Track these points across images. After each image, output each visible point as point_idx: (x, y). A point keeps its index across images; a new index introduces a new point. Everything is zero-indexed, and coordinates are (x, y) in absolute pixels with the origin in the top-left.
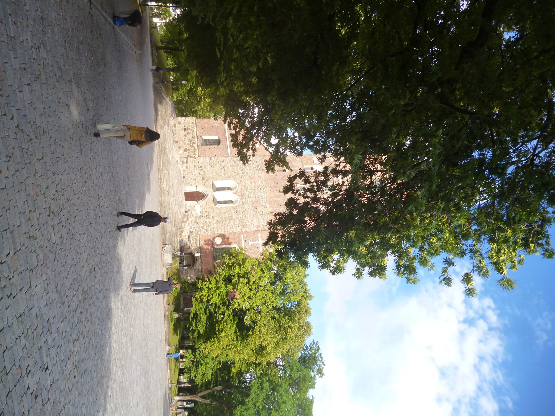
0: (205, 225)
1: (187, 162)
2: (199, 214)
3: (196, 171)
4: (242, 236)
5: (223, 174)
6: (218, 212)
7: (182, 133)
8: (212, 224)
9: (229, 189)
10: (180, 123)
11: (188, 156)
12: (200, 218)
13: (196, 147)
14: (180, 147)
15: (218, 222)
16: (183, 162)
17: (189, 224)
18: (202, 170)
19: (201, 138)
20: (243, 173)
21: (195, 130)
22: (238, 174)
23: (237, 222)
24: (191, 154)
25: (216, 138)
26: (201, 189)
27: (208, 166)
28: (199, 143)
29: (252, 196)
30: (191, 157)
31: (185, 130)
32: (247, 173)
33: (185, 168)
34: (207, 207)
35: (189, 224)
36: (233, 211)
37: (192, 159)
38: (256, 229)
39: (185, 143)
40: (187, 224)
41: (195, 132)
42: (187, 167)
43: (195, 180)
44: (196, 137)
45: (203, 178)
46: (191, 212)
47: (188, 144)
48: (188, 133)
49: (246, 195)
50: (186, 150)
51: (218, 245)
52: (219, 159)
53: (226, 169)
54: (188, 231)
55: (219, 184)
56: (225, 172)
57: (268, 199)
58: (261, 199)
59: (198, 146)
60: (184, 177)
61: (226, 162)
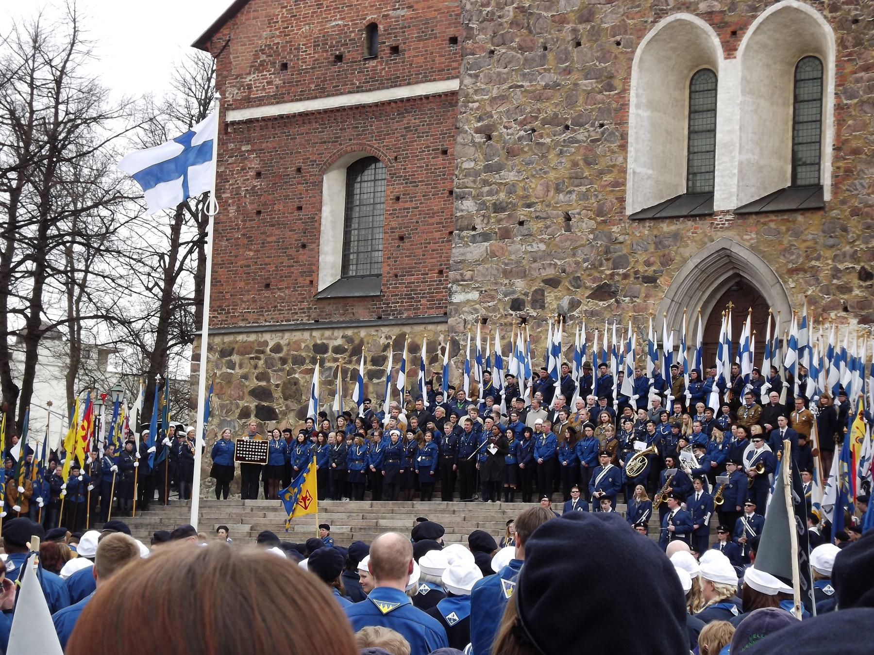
13: (383, 336)
18: (538, 301)
21: (272, 340)
25: (333, 185)
27: (517, 248)
28: (362, 313)
34: (825, 267)
41: (285, 339)
45: (603, 292)
52: (468, 159)
53: (549, 109)
55: (648, 171)
56: (568, 116)
59: (380, 320)
61: (497, 112)
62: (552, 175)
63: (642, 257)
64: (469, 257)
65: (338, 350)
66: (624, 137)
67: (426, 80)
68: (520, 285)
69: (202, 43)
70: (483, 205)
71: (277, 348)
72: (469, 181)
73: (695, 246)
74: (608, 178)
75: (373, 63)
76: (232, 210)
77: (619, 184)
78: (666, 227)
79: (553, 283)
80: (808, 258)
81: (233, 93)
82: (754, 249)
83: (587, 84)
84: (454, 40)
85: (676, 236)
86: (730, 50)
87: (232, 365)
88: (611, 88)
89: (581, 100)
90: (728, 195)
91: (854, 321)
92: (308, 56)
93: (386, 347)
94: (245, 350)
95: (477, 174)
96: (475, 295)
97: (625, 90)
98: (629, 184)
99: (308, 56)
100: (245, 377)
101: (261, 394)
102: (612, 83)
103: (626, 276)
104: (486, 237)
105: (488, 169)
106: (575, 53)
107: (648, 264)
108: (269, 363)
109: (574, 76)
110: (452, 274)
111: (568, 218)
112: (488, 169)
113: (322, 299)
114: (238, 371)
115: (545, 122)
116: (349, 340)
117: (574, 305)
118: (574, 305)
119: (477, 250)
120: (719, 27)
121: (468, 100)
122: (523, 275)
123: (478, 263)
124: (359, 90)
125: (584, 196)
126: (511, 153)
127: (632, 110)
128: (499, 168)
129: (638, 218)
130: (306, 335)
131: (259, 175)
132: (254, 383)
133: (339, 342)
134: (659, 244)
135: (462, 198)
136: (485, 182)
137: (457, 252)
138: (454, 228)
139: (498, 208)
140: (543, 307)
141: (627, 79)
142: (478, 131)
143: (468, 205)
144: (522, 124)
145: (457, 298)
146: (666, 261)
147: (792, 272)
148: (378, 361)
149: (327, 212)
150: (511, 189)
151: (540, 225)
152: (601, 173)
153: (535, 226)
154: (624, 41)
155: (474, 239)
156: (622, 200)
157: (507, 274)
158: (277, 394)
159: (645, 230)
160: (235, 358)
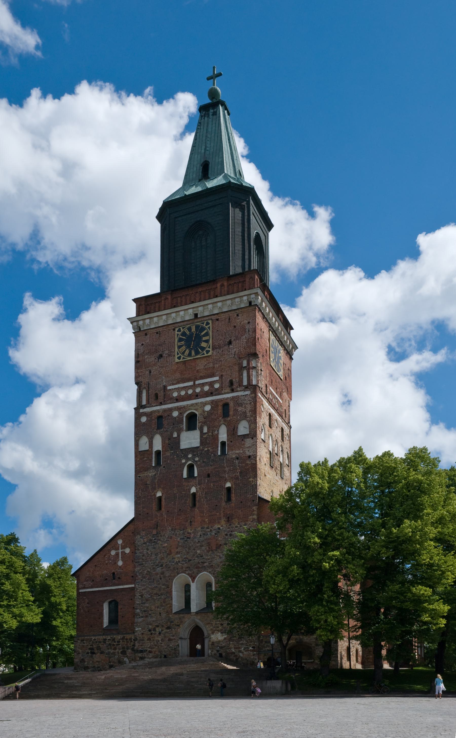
1: (141, 651)
3: (156, 638)
5: (162, 597)
7: (97, 657)
9: (187, 588)
10: (83, 661)
11: (133, 649)
13: (119, 637)
16: (142, 658)
18: (154, 630)
19: (106, 629)
20: (162, 566)
21: (93, 638)
22: (163, 573)
27: (149, 619)
29: (198, 552)
30: (134, 645)
31: (93, 653)
32: (162, 559)
33: (151, 655)
35: (240, 651)
37: (137, 644)
39: (114, 653)
40: (241, 655)
41: (96, 638)
42: (150, 652)
43: (170, 640)
44: (104, 637)
45: (168, 628)
46: (221, 648)
47: (115, 649)
48: (99, 648)
49: (197, 560)
50: (124, 653)
53: (155, 592)
54: (252, 653)
55: (177, 603)
57: (206, 526)
58: (205, 537)
59: (118, 633)
60: (165, 657)
61: (144, 592)
62: (156, 605)
63: (176, 621)
64: (139, 621)
65: (109, 640)
66: (172, 597)
67: (127, 584)
68: (150, 627)
70: (141, 611)
71: (95, 640)
72: (138, 606)
74: (169, 606)
75: (114, 581)
76: (82, 611)
77: (171, 606)
78: (181, 615)
79: (158, 626)
80: (210, 621)
82: (199, 620)
83: (163, 587)
84: (133, 577)
85: (183, 617)
86: (193, 581)
87: (84, 643)
88: (169, 588)
89: (162, 590)
90: (194, 608)
91: (220, 633)
93: (120, 639)
95: (140, 604)
96: (140, 629)
97: (172, 588)
98: (173, 607)
100: (87, 645)
102: (169, 587)
103: (173, 625)
104: (142, 617)
105: (142, 603)
106: (160, 581)
107: (178, 622)
108: (93, 642)
109: (161, 585)
110: (135, 624)
111: (160, 613)
112: (142, 603)
114: (85, 644)
115: (154, 594)
116: (112, 638)
117: (162, 630)
118: (162, 630)
119: (140, 620)
120: (191, 577)
121: (137, 589)
122: (151, 624)
123: (141, 622)
124: (111, 586)
125: (164, 609)
126: (147, 600)
127: (173, 592)
128: (144, 603)
129: (176, 613)
130: (102, 637)
131: (88, 603)
132: (89, 647)
133: (109, 638)
134: (180, 619)
135: (137, 609)
136: (142, 606)
137: (136, 620)
138: (135, 615)
139: (145, 611)
140: (155, 631)
141: (172, 586)
142: (140, 596)
143: (138, 611)
144: (149, 594)
145: (137, 629)
146: (181, 622)
147: (207, 624)
148: (119, 642)
149: (104, 611)
150: (147, 607)
151: (154, 615)
152: (167, 605)
153: (153, 615)
154: (171, 578)
155: (140, 617)
156: (172, 610)
157: (147, 624)
158: (95, 649)
160: (85, 642)
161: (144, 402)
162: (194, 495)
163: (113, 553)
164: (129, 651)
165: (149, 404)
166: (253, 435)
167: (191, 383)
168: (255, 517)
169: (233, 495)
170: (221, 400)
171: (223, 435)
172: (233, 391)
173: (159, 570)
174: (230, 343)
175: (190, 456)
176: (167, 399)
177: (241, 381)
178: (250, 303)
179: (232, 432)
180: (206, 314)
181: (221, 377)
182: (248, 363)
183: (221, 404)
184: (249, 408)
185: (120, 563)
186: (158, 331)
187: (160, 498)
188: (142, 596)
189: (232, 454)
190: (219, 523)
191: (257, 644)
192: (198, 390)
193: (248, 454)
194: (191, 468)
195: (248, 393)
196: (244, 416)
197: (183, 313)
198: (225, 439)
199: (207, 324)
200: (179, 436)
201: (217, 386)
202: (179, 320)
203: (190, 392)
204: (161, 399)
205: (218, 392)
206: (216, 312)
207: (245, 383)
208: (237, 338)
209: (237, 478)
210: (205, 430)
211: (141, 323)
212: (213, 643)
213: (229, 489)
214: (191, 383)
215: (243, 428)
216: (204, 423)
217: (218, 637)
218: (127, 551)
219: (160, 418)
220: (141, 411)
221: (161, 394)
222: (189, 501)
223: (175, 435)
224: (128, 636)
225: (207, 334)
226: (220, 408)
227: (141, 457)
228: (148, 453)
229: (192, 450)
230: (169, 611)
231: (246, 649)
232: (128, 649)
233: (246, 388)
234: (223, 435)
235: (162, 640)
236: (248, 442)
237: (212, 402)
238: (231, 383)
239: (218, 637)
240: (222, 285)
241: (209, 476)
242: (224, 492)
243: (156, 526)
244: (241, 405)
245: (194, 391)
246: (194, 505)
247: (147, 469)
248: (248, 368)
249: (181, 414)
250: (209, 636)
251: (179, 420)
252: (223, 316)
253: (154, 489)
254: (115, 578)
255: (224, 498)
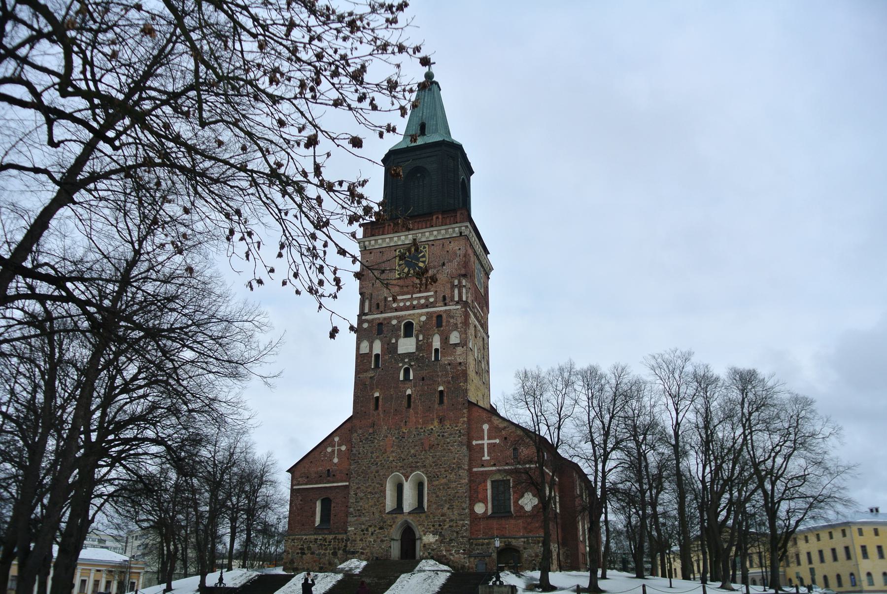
0: (454, 529)
2: (437, 537)
4: (475, 470)
6: (435, 506)
8: (454, 518)
9: (400, 488)
11: (345, 550)
12: (444, 536)
13: (331, 537)
14: (330, 564)
15: (451, 508)
17: (451, 554)
18: (367, 530)
19: (318, 528)
22: (377, 472)
23: (452, 476)
24: (342, 545)
26: (396, 533)
27: (363, 519)
29: (412, 451)
31: (303, 553)
32: (378, 457)
34: (426, 524)
36: (436, 483)
38: (465, 447)
39: (324, 554)
40: (452, 557)
42: (362, 553)
43: (382, 541)
44: (316, 537)
45: (381, 528)
46: (433, 550)
47: (326, 549)
48: (309, 548)
49: (411, 460)
50: (335, 554)
51: (486, 510)
53: (369, 490)
55: (390, 503)
56: (373, 491)
59: (330, 533)
69: (288, 471)
73: (400, 519)
77: (384, 506)
79: (370, 526)
81: (295, 482)
92: (313, 475)
94: (298, 539)
99: (313, 475)
101: (302, 549)
102: (383, 485)
113: (316, 528)
119: (353, 519)
126: (361, 499)
138: (347, 514)
143: (352, 509)
148: (330, 542)
159: (390, 516)
161: (366, 311)
162: (409, 396)
163: (329, 450)
164: (341, 552)
165: (371, 312)
166: (463, 343)
167: (409, 296)
168: (465, 419)
169: (445, 398)
170: (435, 312)
171: (436, 343)
172: (445, 305)
173: (374, 468)
174: (444, 264)
175: (406, 360)
176: (387, 309)
177: (453, 296)
178: (461, 233)
179: (445, 340)
180: (424, 239)
181: (436, 292)
182: (460, 282)
183: (435, 315)
184: (459, 320)
185: (336, 460)
186: (382, 251)
187: (377, 398)
188: (356, 494)
189: (444, 360)
190: (432, 424)
191: (468, 546)
192: (415, 302)
193: (459, 361)
194: (407, 371)
195: (459, 307)
196: (455, 327)
197: (404, 238)
198: (439, 347)
199: (424, 248)
200: (397, 341)
201: (432, 300)
202: (400, 243)
203: (408, 304)
204: (382, 308)
205: (433, 305)
206: (432, 238)
207: (456, 299)
208: (450, 261)
209: (449, 383)
210: (421, 338)
211: (367, 243)
212: (425, 545)
213: (441, 392)
214: (409, 296)
215: (454, 338)
216: (420, 332)
217: (430, 539)
218: (343, 448)
219: (380, 324)
220: (364, 317)
221: (382, 304)
222: (405, 402)
223: (393, 341)
224: (340, 537)
225: (424, 256)
226: (434, 319)
227: (362, 360)
228: (368, 355)
229: (409, 355)
230: (382, 511)
231: (457, 552)
232: (339, 549)
233: (457, 303)
234: (436, 343)
235: (374, 541)
236: (459, 350)
237: (428, 313)
238: (444, 298)
239: (430, 539)
240: (437, 218)
241: (423, 379)
242: (437, 395)
243: (373, 425)
244: (453, 317)
245: (412, 303)
246: (409, 406)
247: (366, 371)
248: (460, 287)
249: (399, 322)
250: (420, 539)
251: (396, 328)
252: (437, 242)
253: (372, 389)
254: (329, 475)
255: (437, 400)
